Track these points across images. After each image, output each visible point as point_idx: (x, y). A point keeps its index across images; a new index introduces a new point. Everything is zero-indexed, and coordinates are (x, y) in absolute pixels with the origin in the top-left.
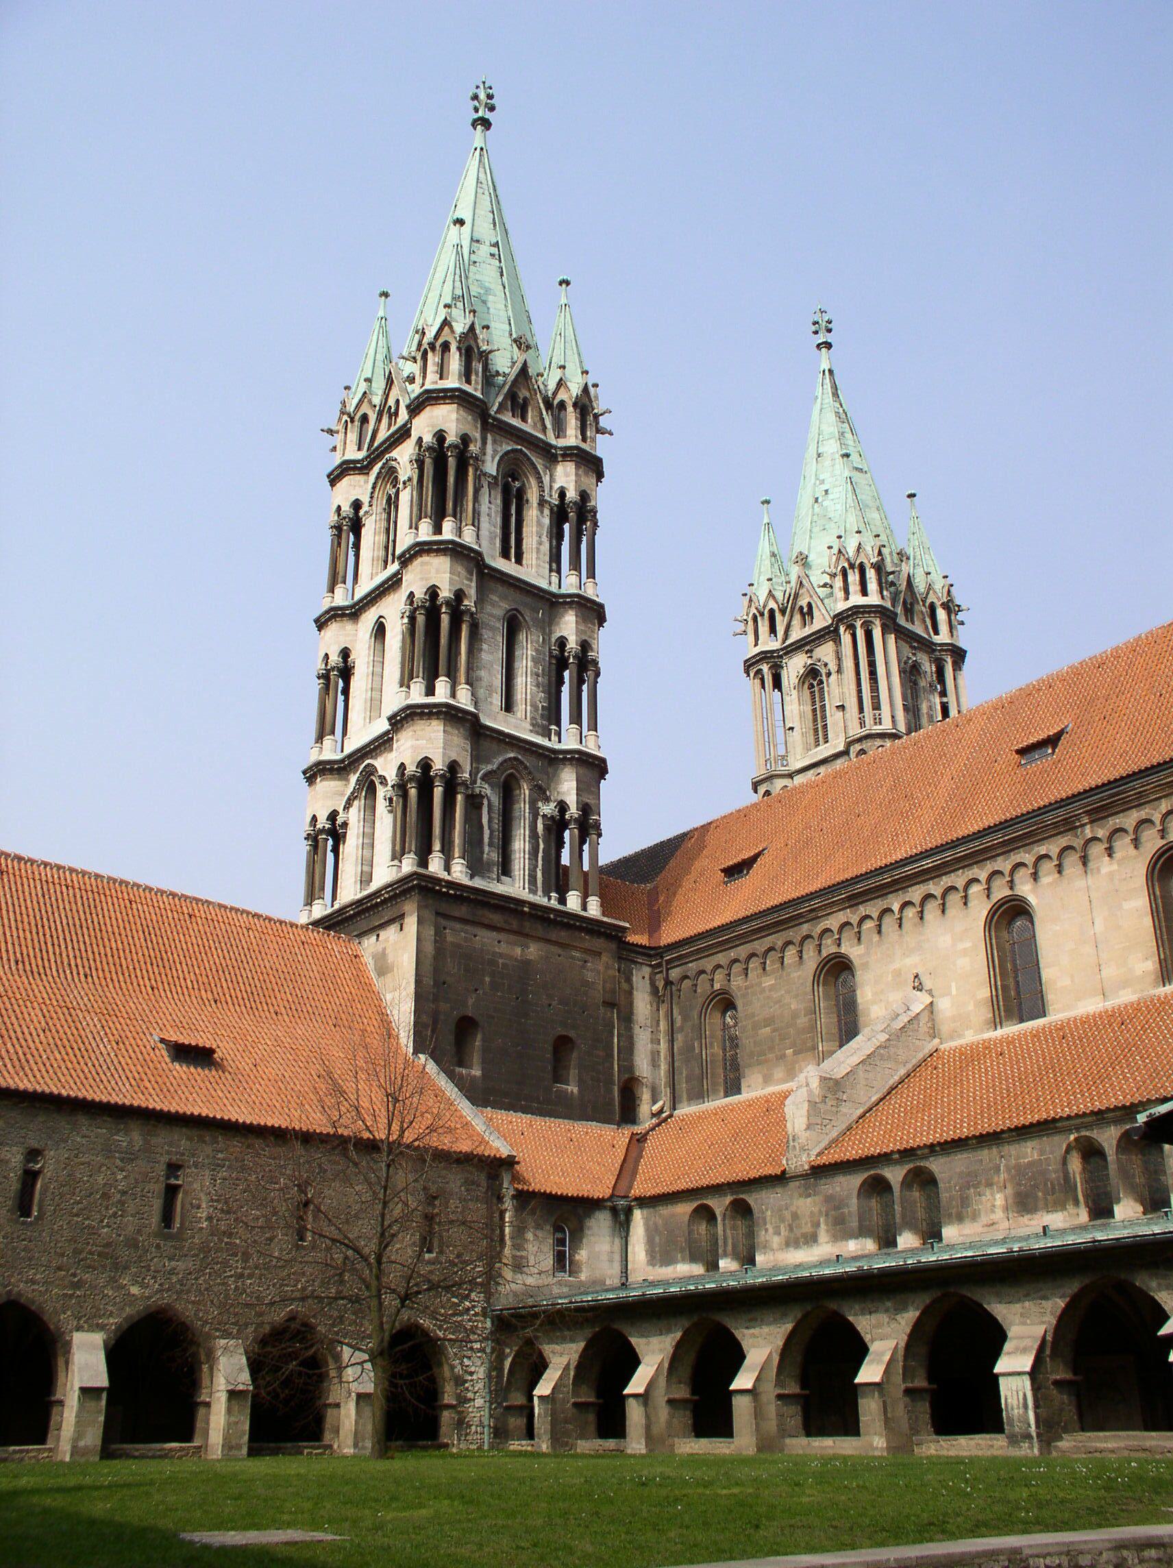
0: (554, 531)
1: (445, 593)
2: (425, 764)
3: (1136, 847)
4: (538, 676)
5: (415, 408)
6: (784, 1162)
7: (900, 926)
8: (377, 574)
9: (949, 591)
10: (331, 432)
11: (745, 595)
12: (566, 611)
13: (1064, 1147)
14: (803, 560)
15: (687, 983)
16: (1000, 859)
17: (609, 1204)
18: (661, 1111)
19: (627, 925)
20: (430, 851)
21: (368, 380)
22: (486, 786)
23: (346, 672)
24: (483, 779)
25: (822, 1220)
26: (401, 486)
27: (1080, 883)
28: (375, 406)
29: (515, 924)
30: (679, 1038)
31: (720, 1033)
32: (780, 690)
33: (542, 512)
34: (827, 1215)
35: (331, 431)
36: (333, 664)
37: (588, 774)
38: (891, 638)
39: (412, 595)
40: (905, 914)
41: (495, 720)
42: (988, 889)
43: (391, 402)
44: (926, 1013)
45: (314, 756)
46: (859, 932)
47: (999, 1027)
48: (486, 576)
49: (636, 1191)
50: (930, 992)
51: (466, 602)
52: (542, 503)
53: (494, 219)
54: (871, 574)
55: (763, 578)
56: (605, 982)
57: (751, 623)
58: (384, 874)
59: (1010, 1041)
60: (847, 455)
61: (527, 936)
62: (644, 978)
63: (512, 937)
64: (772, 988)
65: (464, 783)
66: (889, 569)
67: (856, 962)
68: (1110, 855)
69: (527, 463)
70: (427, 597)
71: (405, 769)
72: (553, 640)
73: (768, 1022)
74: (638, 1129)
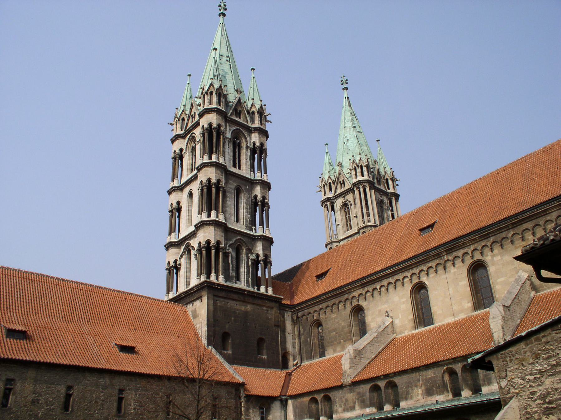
0: (252, 157)
1: (214, 181)
2: (208, 242)
3: (463, 263)
4: (248, 209)
5: (201, 115)
6: (342, 381)
7: (380, 294)
8: (189, 174)
9: (393, 174)
10: (171, 124)
11: (320, 178)
13: (442, 371)
14: (340, 165)
15: (304, 317)
16: (415, 269)
17: (279, 398)
18: (297, 364)
19: (282, 297)
20: (211, 273)
21: (184, 106)
22: (230, 249)
23: (179, 210)
24: (229, 246)
25: (356, 401)
26: (197, 143)
27: (444, 276)
28: (187, 115)
29: (242, 299)
30: (302, 337)
31: (317, 335)
32: (334, 211)
33: (247, 151)
36: (174, 207)
38: (373, 191)
39: (202, 181)
40: (381, 290)
41: (233, 225)
42: (411, 280)
43: (193, 113)
44: (391, 325)
45: (168, 240)
46: (365, 297)
47: (417, 329)
48: (228, 174)
49: (289, 393)
50: (392, 317)
51: (221, 184)
52: (247, 147)
53: (227, 48)
54: (365, 169)
55: (327, 172)
56: (275, 318)
57: (323, 188)
58: (194, 282)
59: (421, 334)
60: (355, 127)
62: (289, 316)
63: (241, 303)
64: (335, 318)
65: (222, 248)
66: (371, 167)
67: (365, 308)
68: (454, 266)
70: (207, 182)
71: (201, 244)
72: (253, 196)
73: (334, 330)
74: (289, 371)
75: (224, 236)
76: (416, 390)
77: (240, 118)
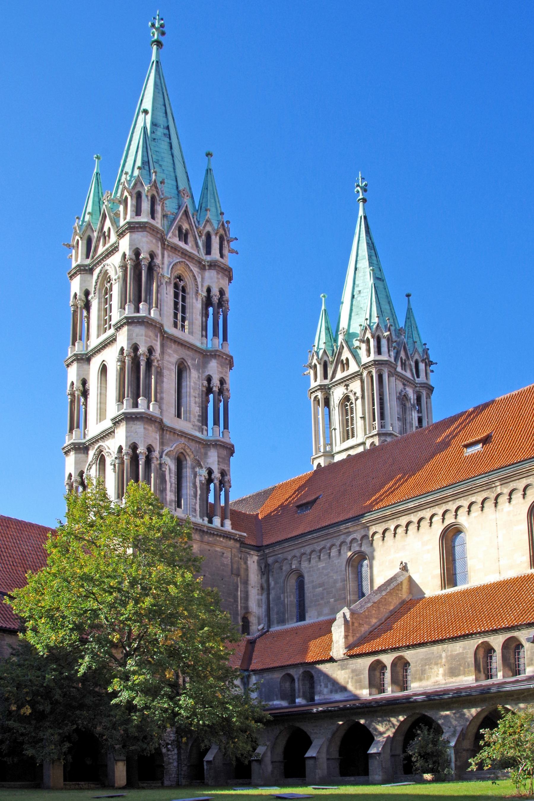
0: (204, 312)
5: (121, 235)
12: (211, 360)
22: (168, 459)
24: (166, 455)
25: (350, 681)
34: (352, 678)
37: (224, 452)
59: (448, 596)
72: (204, 377)
75: (158, 437)
76: (436, 670)
77: (186, 242)
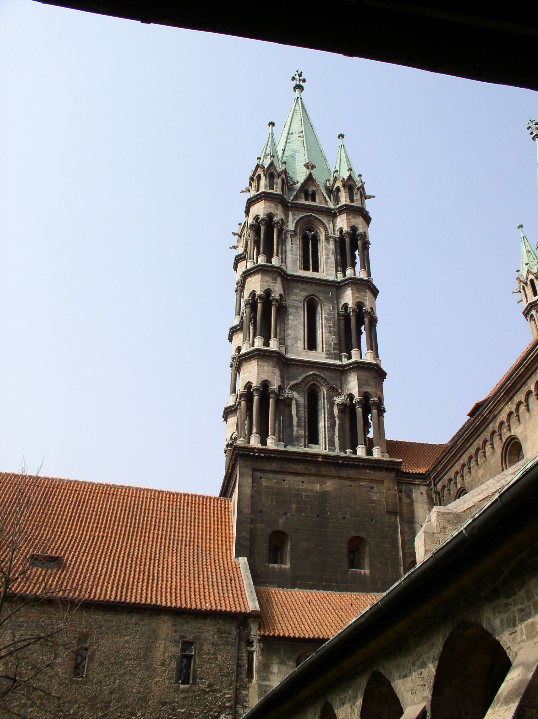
29: (313, 470)
35: (234, 246)
41: (300, 355)
56: (387, 498)
61: (324, 476)
62: (422, 493)
63: (313, 478)
65: (273, 392)
67: (520, 438)
69: (317, 221)
70: (251, 298)
